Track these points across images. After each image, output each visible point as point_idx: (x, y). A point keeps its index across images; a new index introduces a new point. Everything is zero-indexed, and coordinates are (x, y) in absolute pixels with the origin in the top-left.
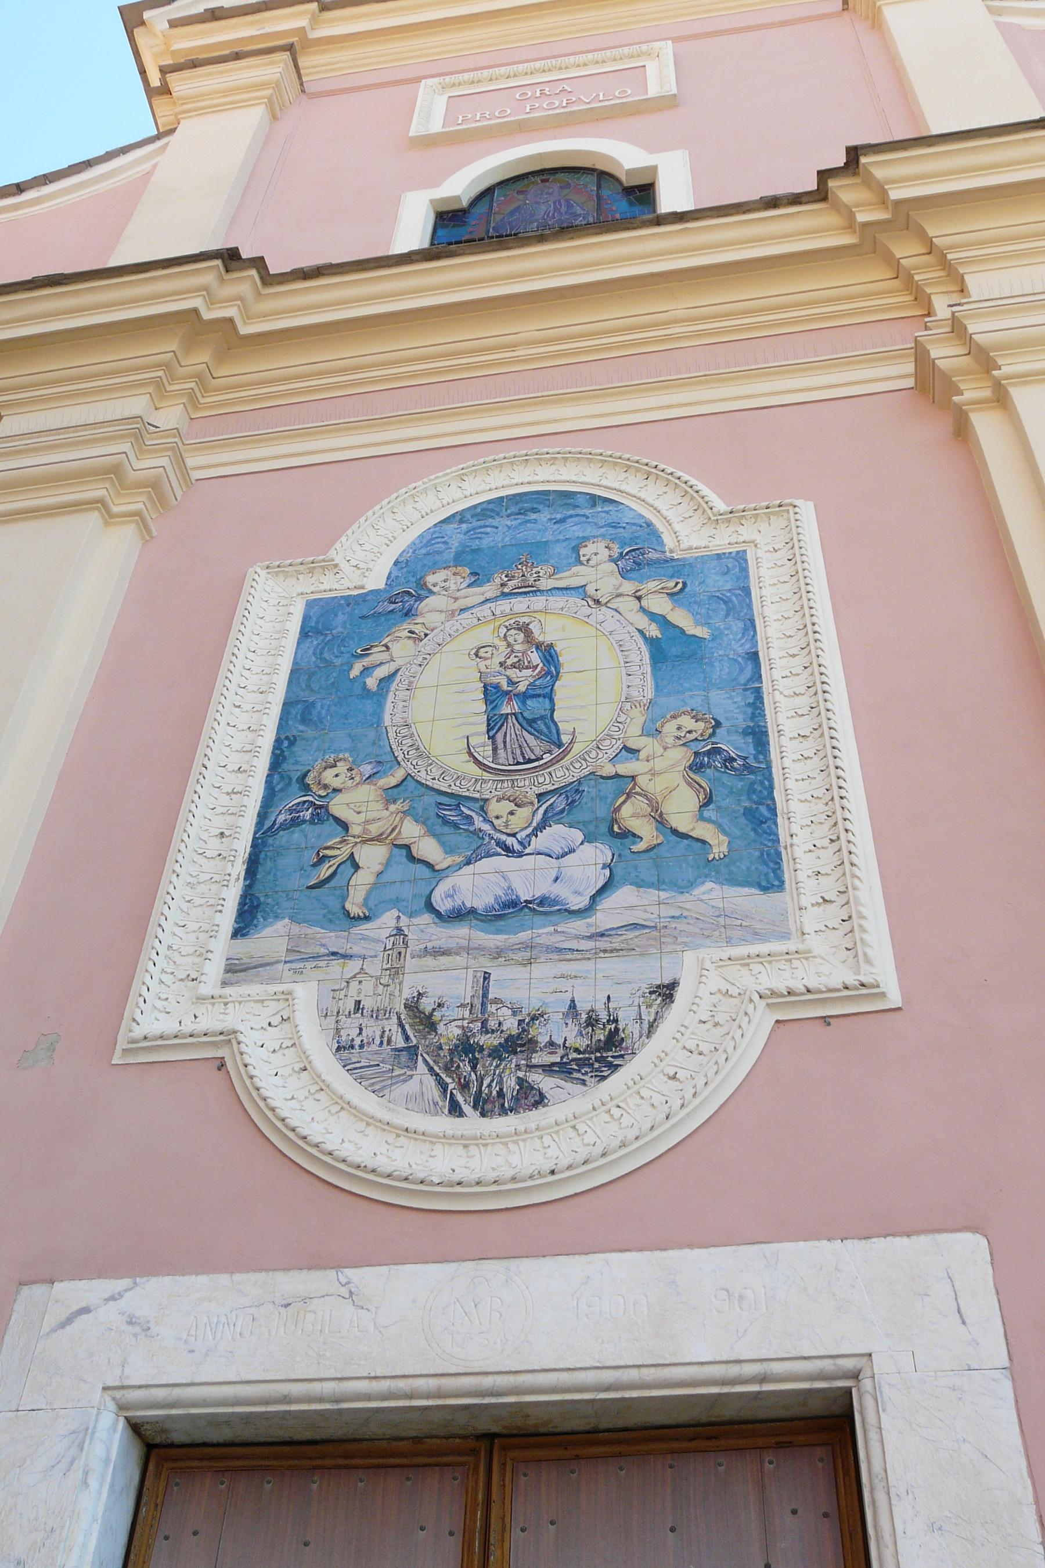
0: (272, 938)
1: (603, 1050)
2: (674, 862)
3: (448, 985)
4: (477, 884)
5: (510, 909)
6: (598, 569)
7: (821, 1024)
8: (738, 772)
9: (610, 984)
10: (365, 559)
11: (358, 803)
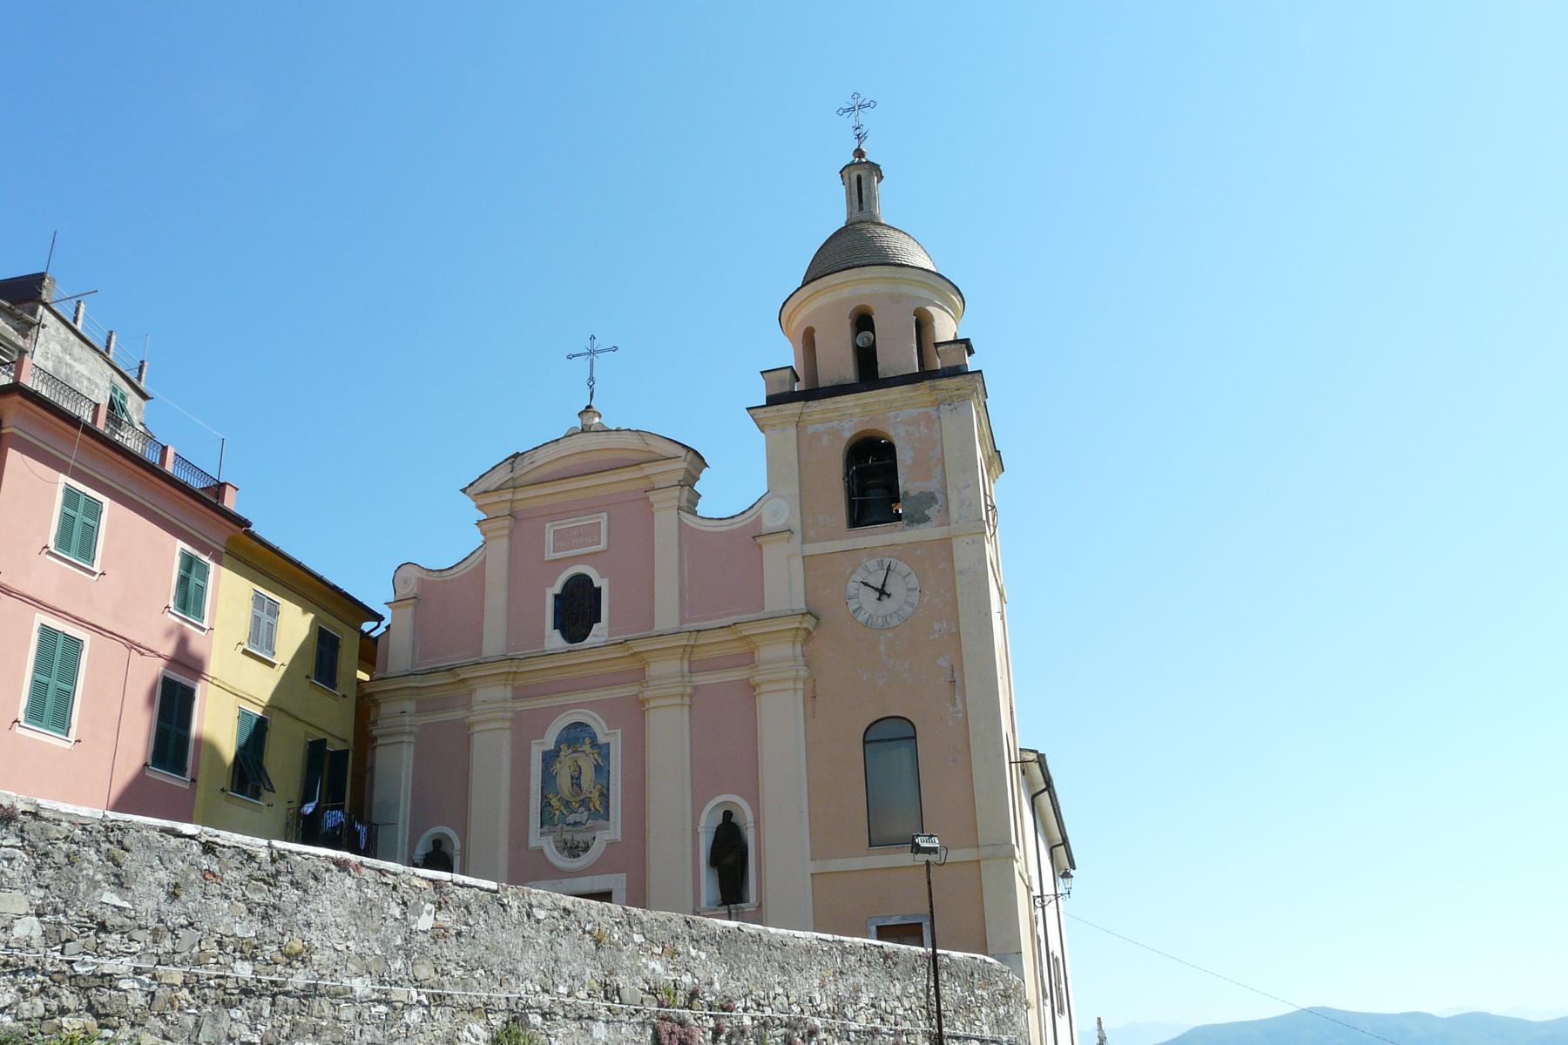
0: (546, 828)
1: (587, 848)
2: (594, 815)
3: (568, 837)
4: (571, 818)
5: (575, 824)
6: (587, 748)
7: (611, 845)
8: (605, 796)
9: (587, 837)
10: (549, 742)
11: (554, 802)
